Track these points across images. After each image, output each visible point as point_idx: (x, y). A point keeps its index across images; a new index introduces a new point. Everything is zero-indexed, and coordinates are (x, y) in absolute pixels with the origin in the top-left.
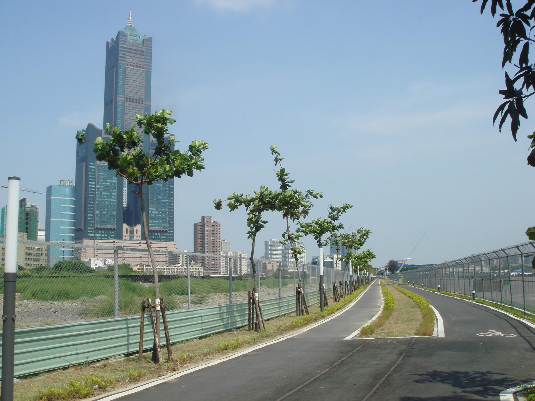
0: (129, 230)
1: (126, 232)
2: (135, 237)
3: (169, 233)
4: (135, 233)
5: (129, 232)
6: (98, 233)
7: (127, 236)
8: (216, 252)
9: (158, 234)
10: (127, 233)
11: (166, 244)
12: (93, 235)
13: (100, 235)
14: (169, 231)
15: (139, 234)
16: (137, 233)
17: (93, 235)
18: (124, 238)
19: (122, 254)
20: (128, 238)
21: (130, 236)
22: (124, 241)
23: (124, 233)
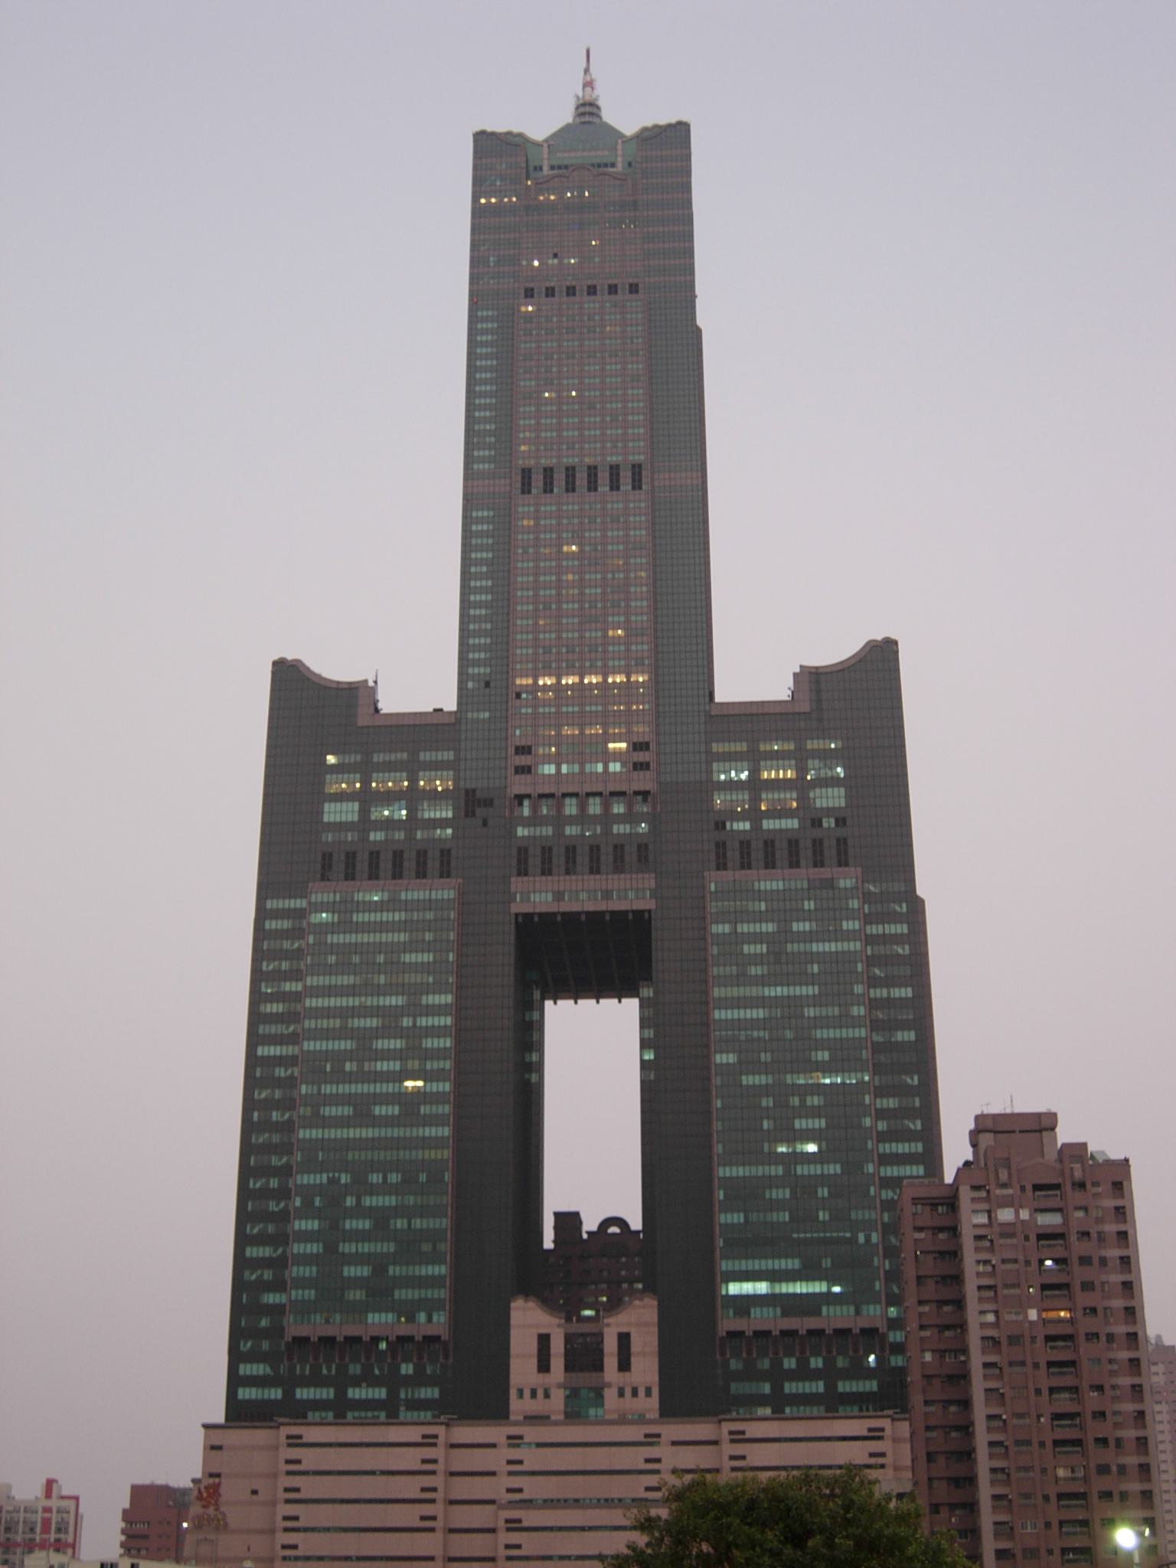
0: (557, 1346)
1: (533, 1363)
2: (610, 1394)
4: (611, 1362)
5: (557, 1363)
6: (316, 1381)
8: (1103, 1442)
9: (803, 1363)
10: (544, 1366)
12: (276, 1394)
13: (327, 1393)
15: (646, 1369)
16: (624, 1365)
17: (276, 1394)
18: (518, 1406)
21: (573, 1394)
23: (522, 1369)
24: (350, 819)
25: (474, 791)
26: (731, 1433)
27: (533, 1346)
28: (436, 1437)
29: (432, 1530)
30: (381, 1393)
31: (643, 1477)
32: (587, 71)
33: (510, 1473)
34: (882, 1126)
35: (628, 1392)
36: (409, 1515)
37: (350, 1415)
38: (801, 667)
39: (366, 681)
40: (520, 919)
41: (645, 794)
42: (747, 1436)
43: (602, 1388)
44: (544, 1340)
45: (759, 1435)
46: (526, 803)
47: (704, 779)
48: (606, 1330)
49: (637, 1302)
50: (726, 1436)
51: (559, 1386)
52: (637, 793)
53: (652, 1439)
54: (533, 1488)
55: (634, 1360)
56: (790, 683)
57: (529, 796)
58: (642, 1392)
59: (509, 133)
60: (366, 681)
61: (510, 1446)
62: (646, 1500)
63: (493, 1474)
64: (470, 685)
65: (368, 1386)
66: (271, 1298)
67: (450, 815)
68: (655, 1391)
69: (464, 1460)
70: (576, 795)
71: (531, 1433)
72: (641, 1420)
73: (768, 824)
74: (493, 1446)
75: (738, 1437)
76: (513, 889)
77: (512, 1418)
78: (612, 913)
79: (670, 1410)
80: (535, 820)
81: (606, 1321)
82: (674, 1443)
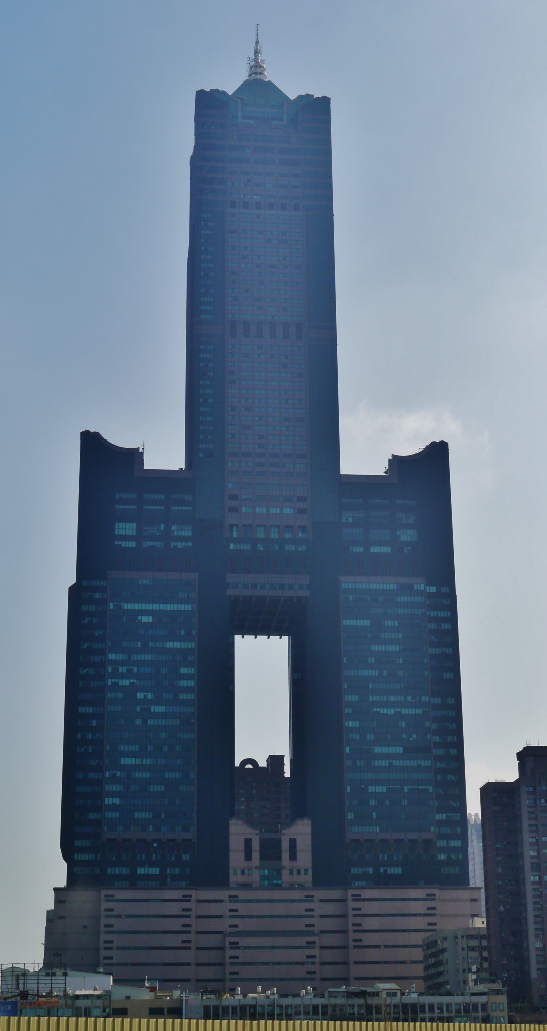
0: (256, 845)
1: (242, 855)
2: (285, 873)
3: (442, 850)
4: (285, 855)
5: (256, 856)
7: (250, 869)
10: (248, 857)
11: (431, 897)
13: (125, 871)
14: (442, 843)
16: (293, 857)
18: (234, 878)
19: (222, 948)
20: (256, 877)
22: (233, 893)
24: (131, 533)
26: (353, 895)
27: (242, 846)
28: (190, 896)
29: (189, 948)
30: (155, 871)
31: (304, 919)
32: (257, 42)
33: (231, 917)
34: (434, 726)
35: (295, 872)
36: (175, 941)
37: (139, 883)
38: (393, 456)
39: (139, 448)
41: (304, 529)
42: (362, 897)
43: (281, 870)
44: (248, 842)
45: (368, 897)
46: (235, 529)
48: (283, 837)
49: (299, 822)
50: (350, 897)
51: (257, 868)
52: (299, 527)
53: (309, 898)
54: (243, 925)
55: (299, 855)
56: (386, 464)
57: (237, 525)
58: (302, 872)
59: (217, 90)
60: (139, 448)
61: (230, 901)
62: (306, 931)
63: (221, 917)
65: (149, 867)
66: (92, 816)
67: (190, 534)
68: (310, 872)
69: (206, 909)
70: (264, 526)
71: (242, 894)
72: (302, 887)
73: (374, 549)
74: (221, 901)
75: (357, 898)
77: (231, 886)
79: (318, 882)
81: (283, 832)
82: (321, 901)
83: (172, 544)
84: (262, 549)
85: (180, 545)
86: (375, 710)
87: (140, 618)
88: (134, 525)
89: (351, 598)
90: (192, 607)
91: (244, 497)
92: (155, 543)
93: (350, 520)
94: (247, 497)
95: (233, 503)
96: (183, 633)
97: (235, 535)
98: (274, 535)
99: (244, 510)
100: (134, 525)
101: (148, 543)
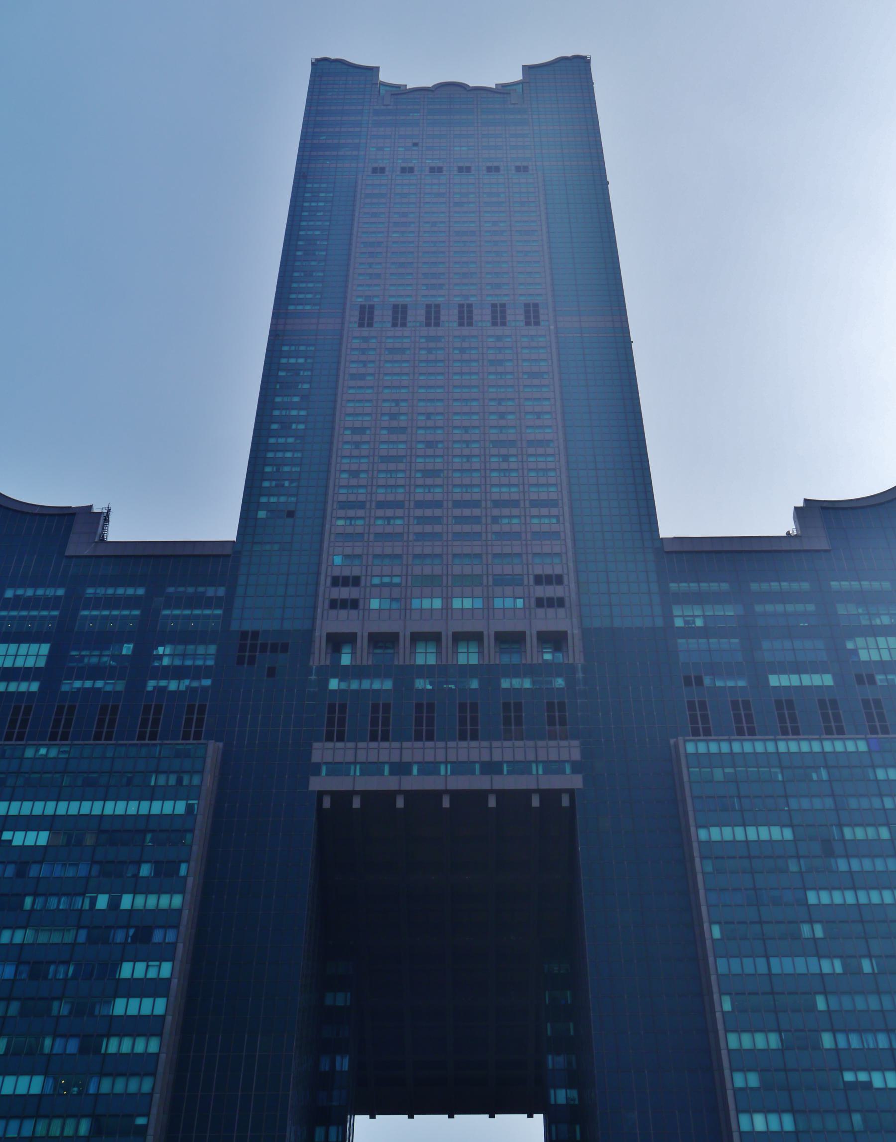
24: (30, 663)
25: (255, 634)
38: (806, 500)
40: (326, 803)
47: (659, 622)
64: (262, 514)
76: (316, 757)
78: (501, 794)
80: (356, 672)
83: (151, 684)
84: (429, 687)
85: (173, 686)
86: (849, 1077)
87: (7, 836)
88: (45, 648)
89: (718, 774)
90: (189, 808)
91: (376, 581)
92: (99, 684)
93: (699, 623)
94: (386, 580)
95: (345, 593)
96: (145, 870)
97: (346, 659)
98: (468, 656)
99: (375, 604)
100: (45, 648)
101: (77, 684)
